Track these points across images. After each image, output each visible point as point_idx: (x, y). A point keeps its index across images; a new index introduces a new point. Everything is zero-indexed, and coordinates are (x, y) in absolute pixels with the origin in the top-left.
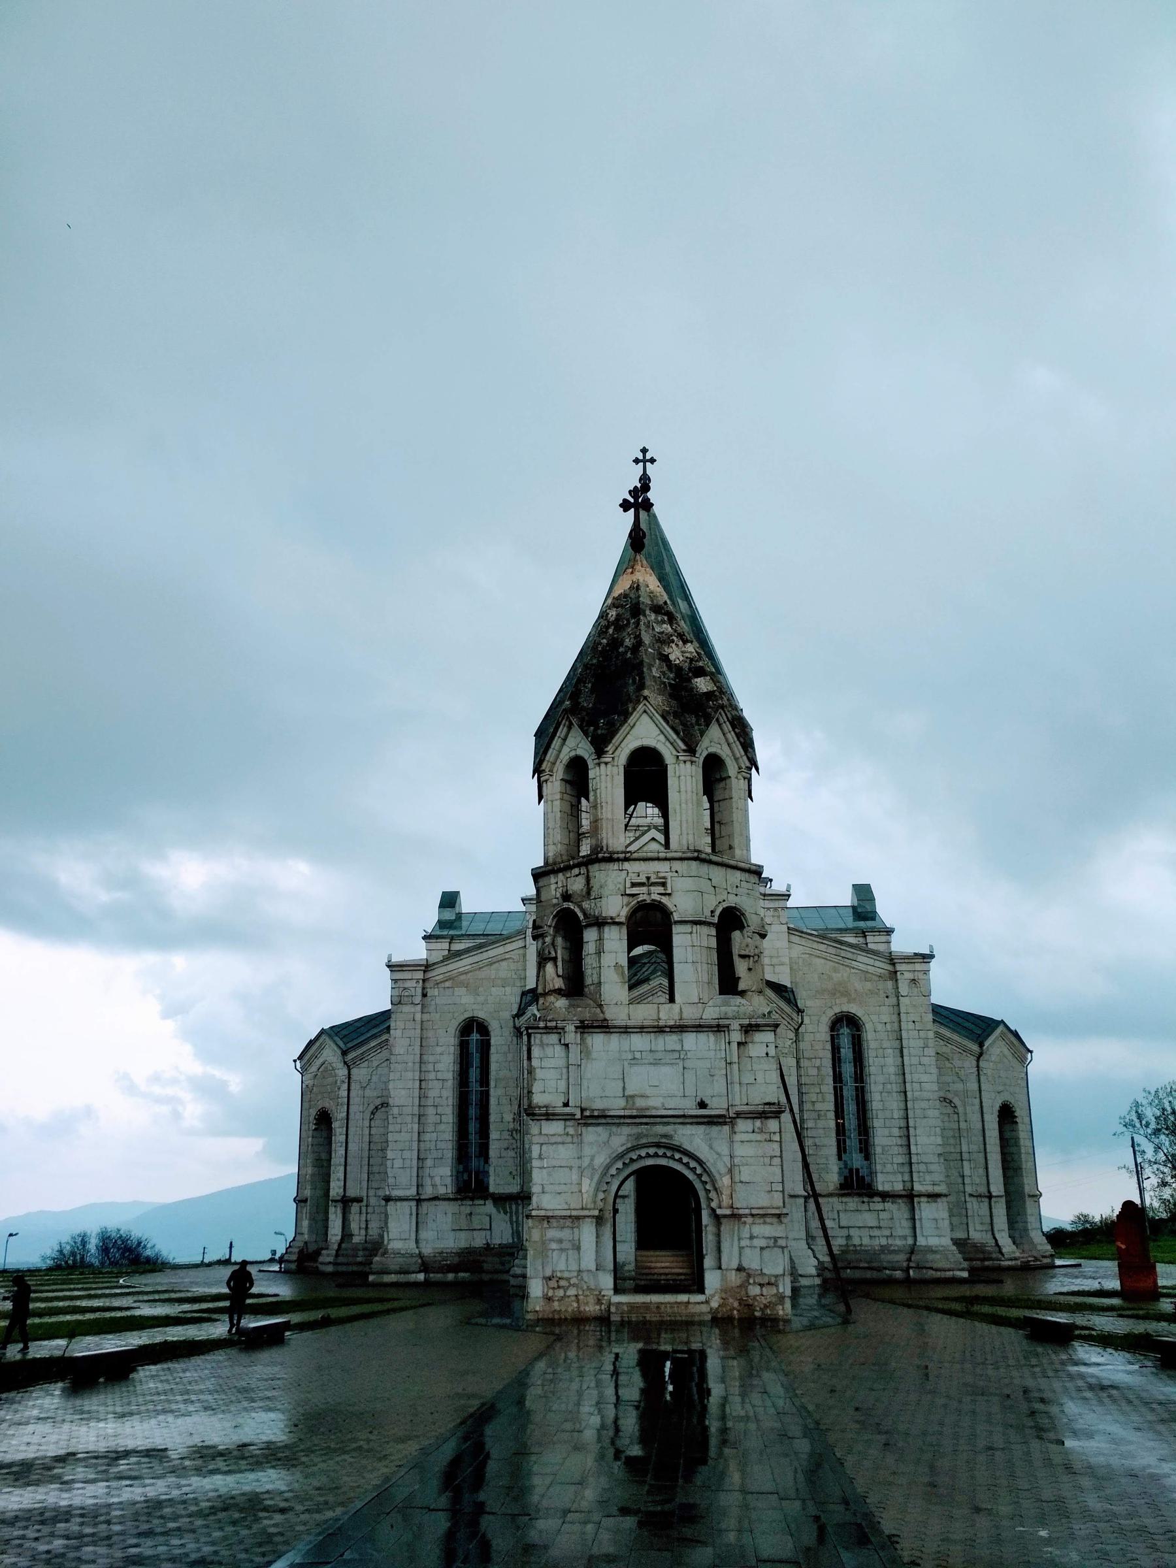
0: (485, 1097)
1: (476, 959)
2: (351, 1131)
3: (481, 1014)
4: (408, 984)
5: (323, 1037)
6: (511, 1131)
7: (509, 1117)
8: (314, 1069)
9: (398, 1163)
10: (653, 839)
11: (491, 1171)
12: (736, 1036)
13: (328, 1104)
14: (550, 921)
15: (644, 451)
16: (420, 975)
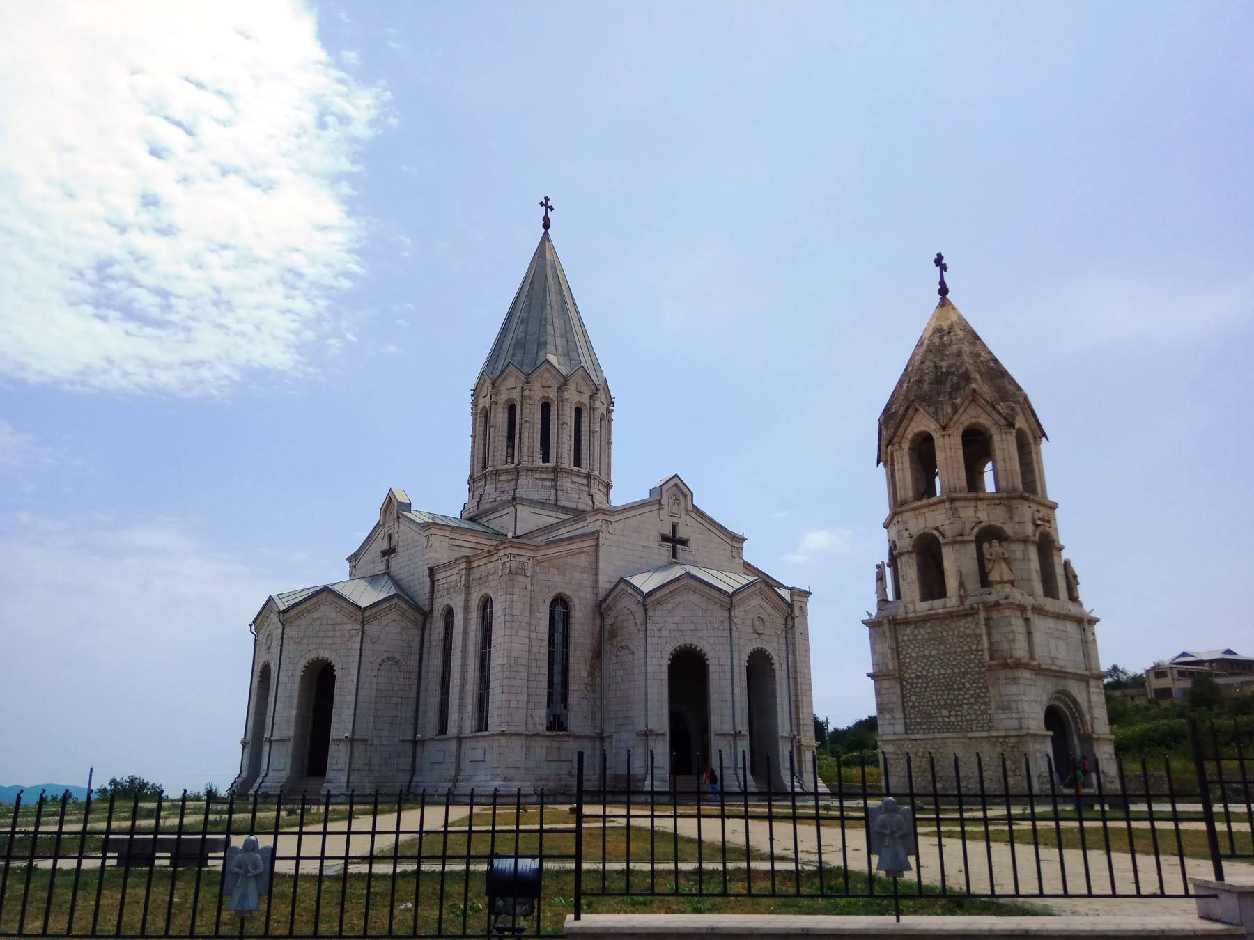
0: (566, 657)
1: (565, 548)
2: (362, 678)
3: (567, 592)
4: (525, 560)
5: (324, 595)
6: (586, 685)
7: (584, 674)
8: (303, 621)
9: (513, 704)
10: (676, 485)
11: (571, 715)
12: (1086, 625)
13: (326, 654)
14: (975, 531)
15: (547, 199)
16: (531, 554)
